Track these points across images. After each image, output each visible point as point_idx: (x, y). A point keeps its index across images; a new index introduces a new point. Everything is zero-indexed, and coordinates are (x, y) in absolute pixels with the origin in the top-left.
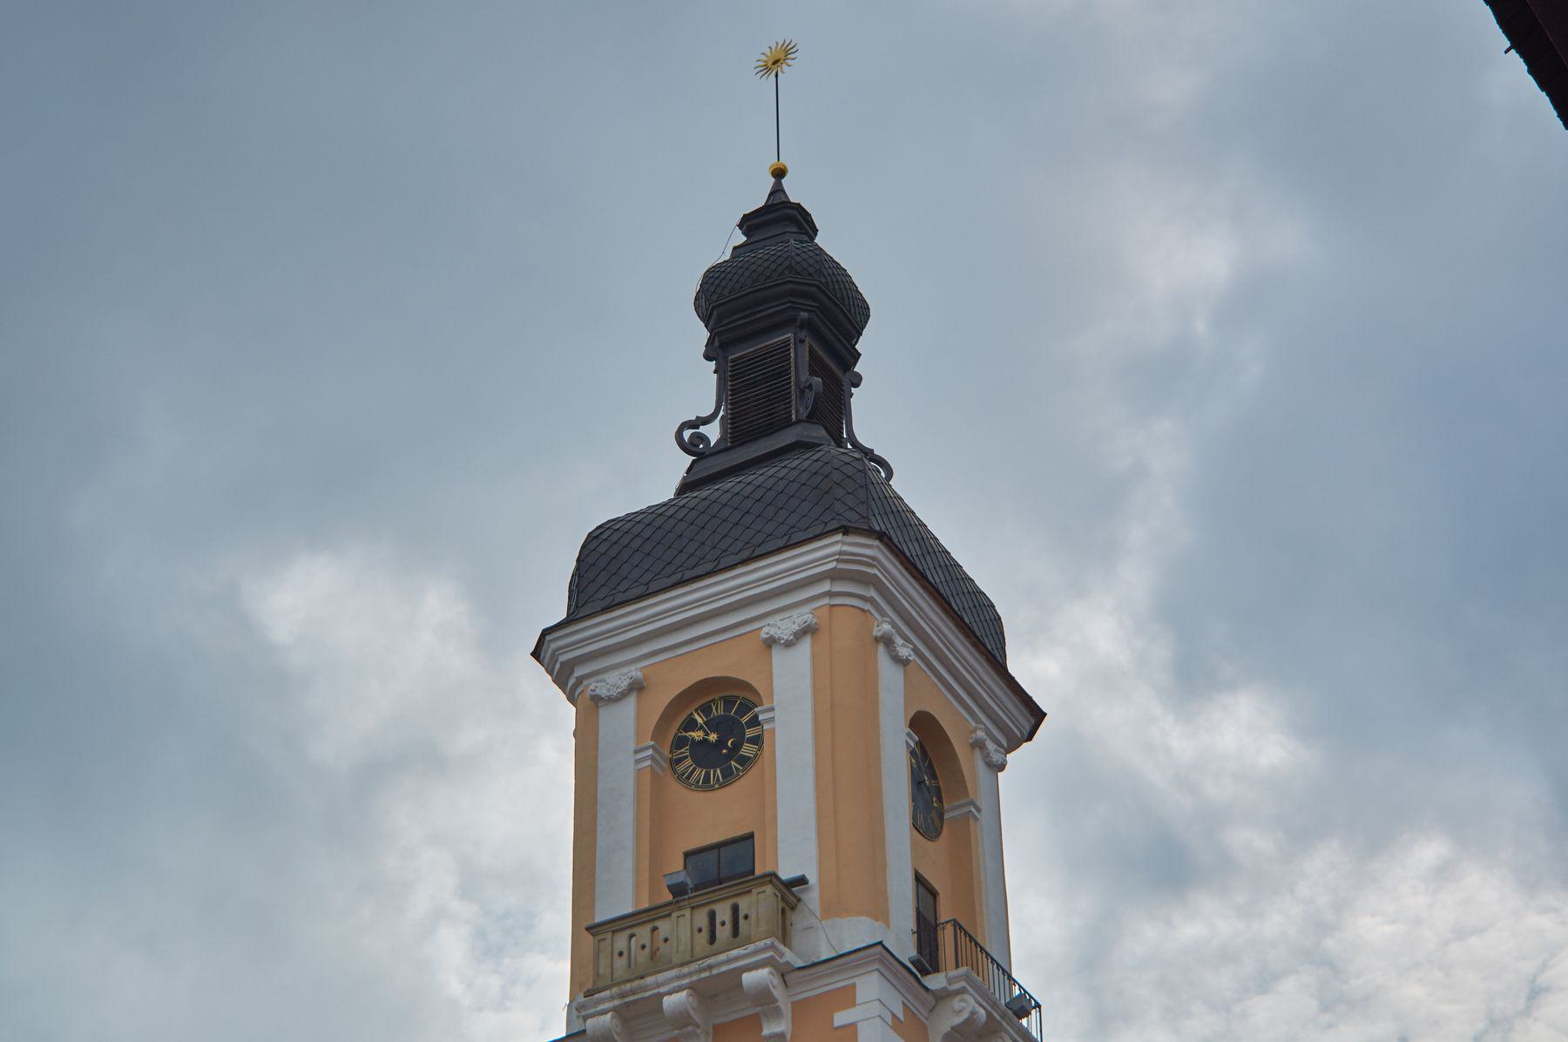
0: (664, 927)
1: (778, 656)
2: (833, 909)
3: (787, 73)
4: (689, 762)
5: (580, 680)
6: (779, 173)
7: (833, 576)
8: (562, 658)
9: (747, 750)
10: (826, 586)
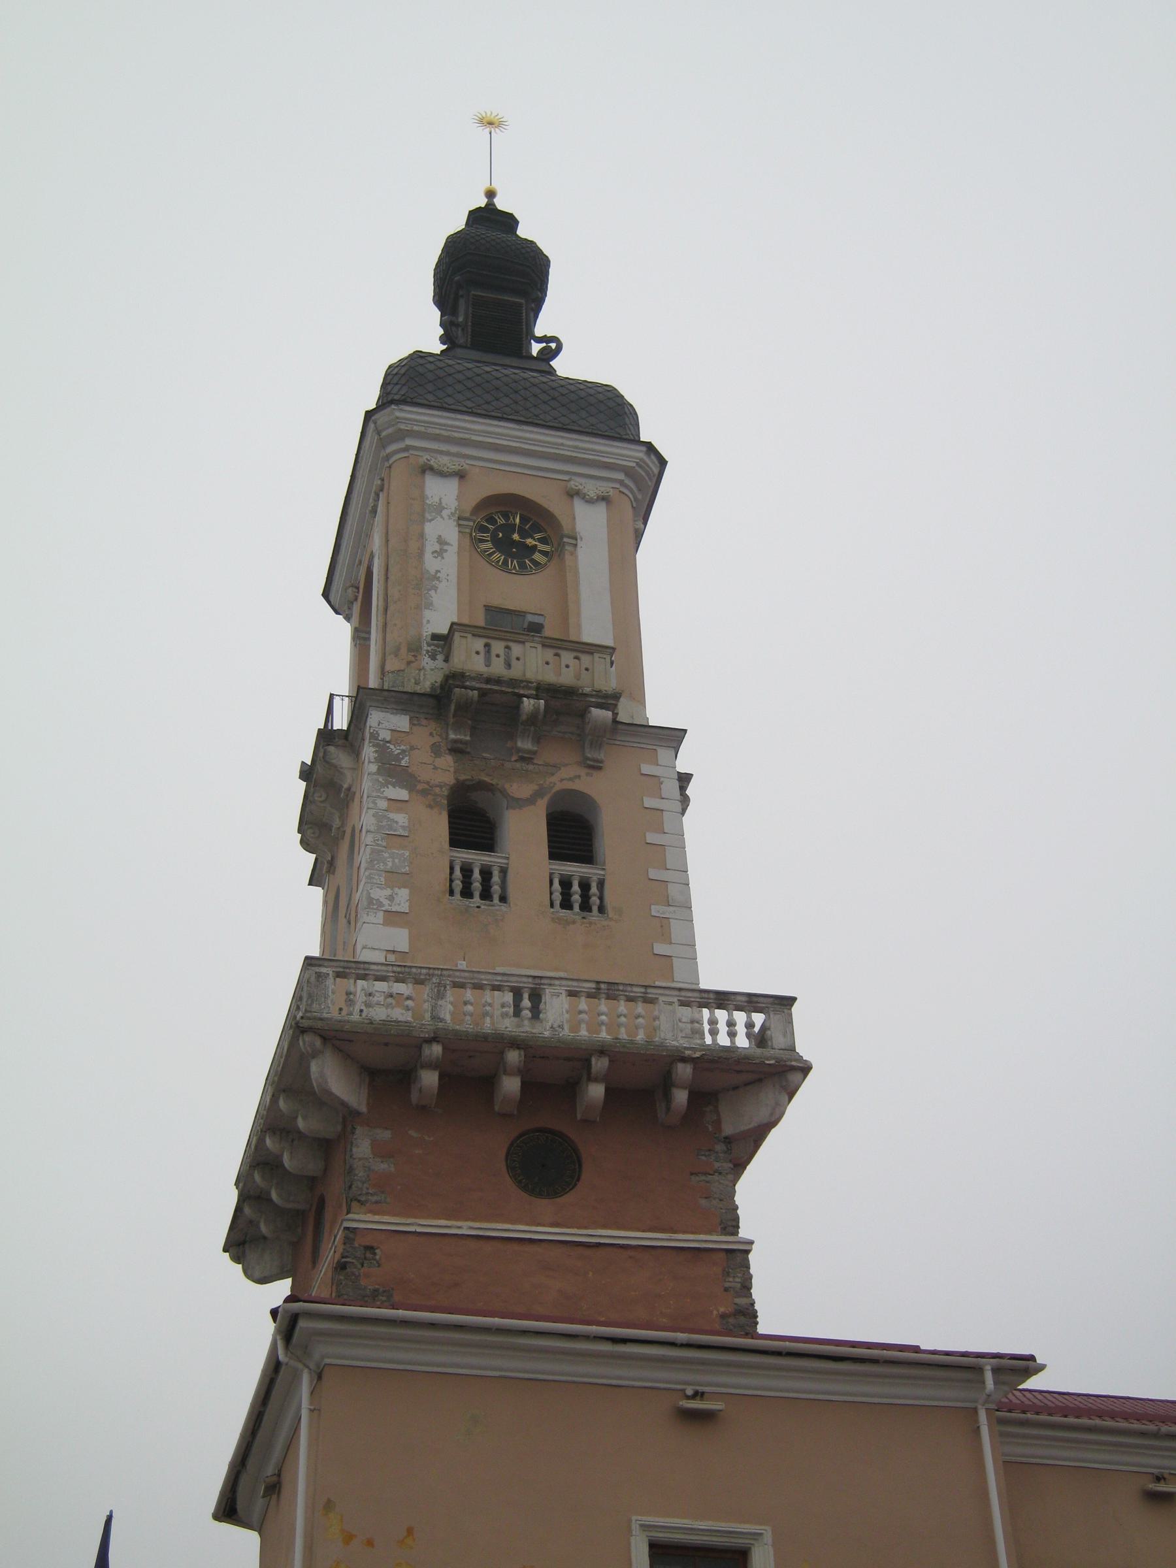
0: (516, 649)
1: (579, 507)
3: (497, 135)
4: (489, 545)
5: (407, 449)
6: (491, 194)
8: (403, 427)
9: (537, 557)
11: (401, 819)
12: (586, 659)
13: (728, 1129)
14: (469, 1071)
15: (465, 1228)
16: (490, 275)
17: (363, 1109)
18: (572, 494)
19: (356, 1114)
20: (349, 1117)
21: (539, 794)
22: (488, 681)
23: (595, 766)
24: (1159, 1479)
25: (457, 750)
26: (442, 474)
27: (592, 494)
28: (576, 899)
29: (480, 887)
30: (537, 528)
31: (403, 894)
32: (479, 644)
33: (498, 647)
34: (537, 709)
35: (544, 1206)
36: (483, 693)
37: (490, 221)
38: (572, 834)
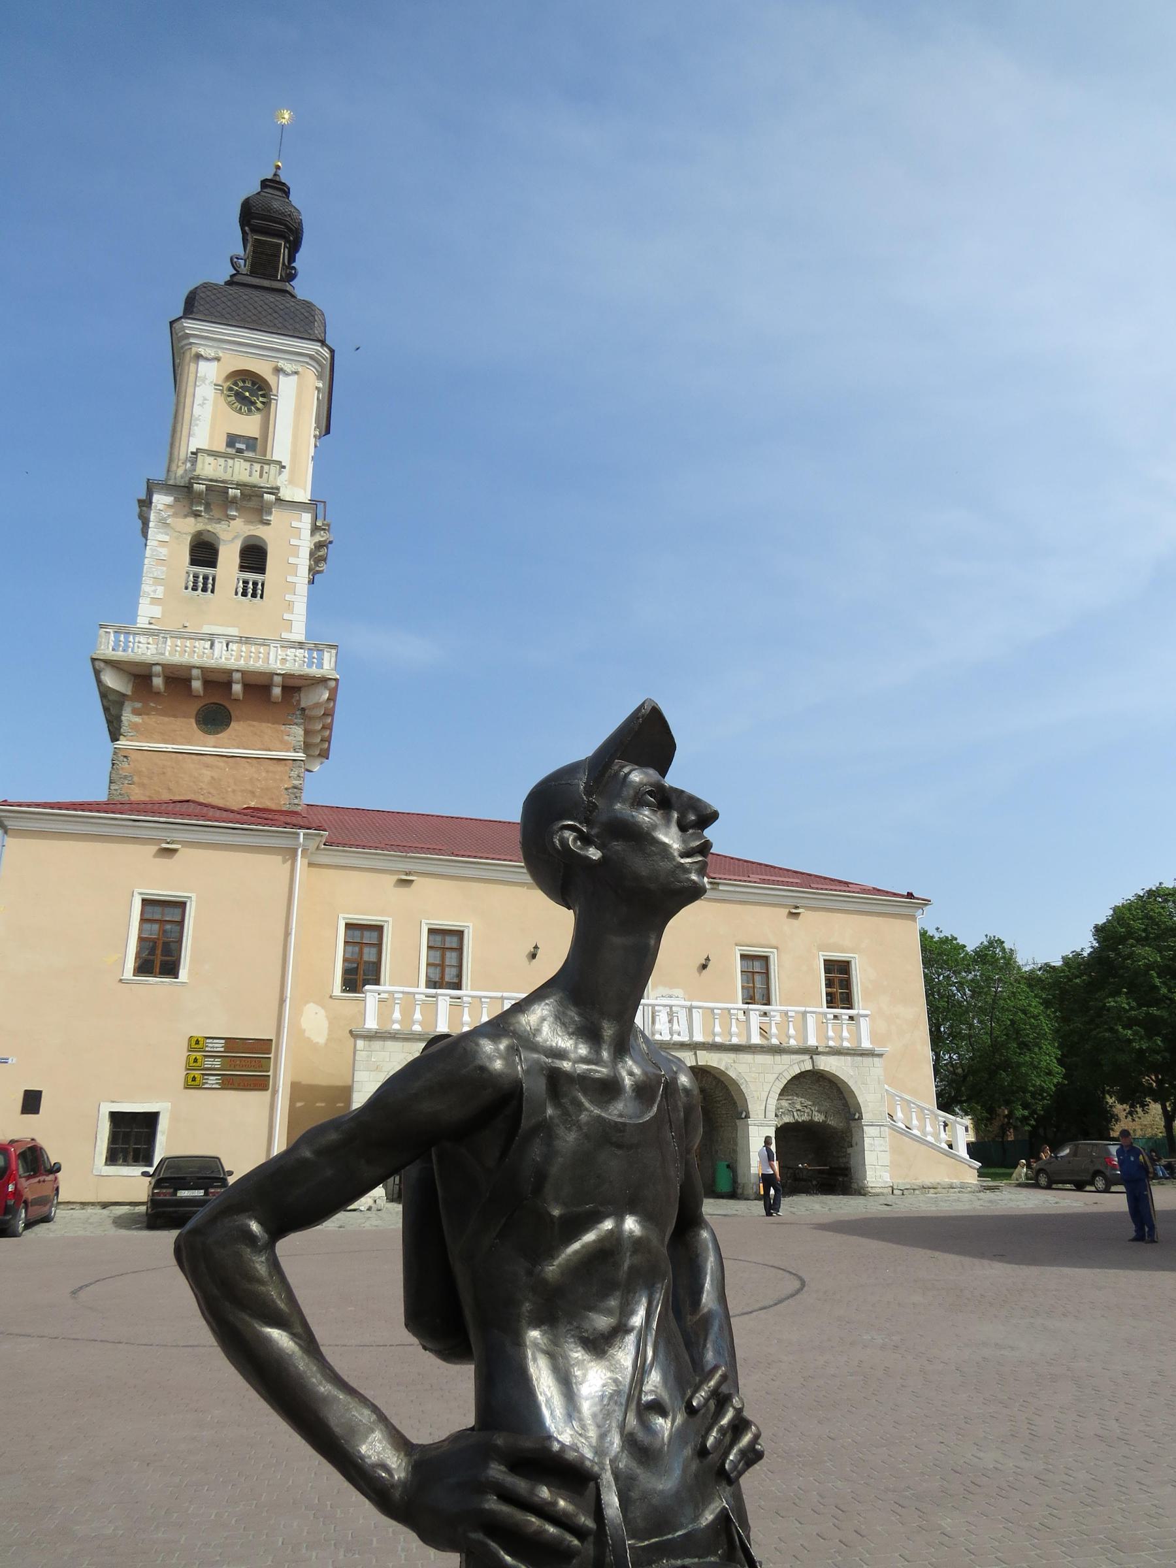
2: (291, 481)
7: (311, 357)
10: (307, 360)
11: (164, 552)
12: (266, 467)
13: (303, 705)
14: (178, 679)
15: (170, 747)
17: (129, 693)
18: (278, 371)
19: (124, 695)
21: (235, 538)
22: (211, 480)
23: (268, 523)
25: (197, 515)
26: (207, 359)
27: (289, 371)
28: (252, 591)
30: (260, 388)
31: (160, 589)
32: (210, 459)
33: (221, 461)
34: (235, 497)
35: (211, 739)
36: (208, 488)
37: (274, 185)
38: (254, 557)
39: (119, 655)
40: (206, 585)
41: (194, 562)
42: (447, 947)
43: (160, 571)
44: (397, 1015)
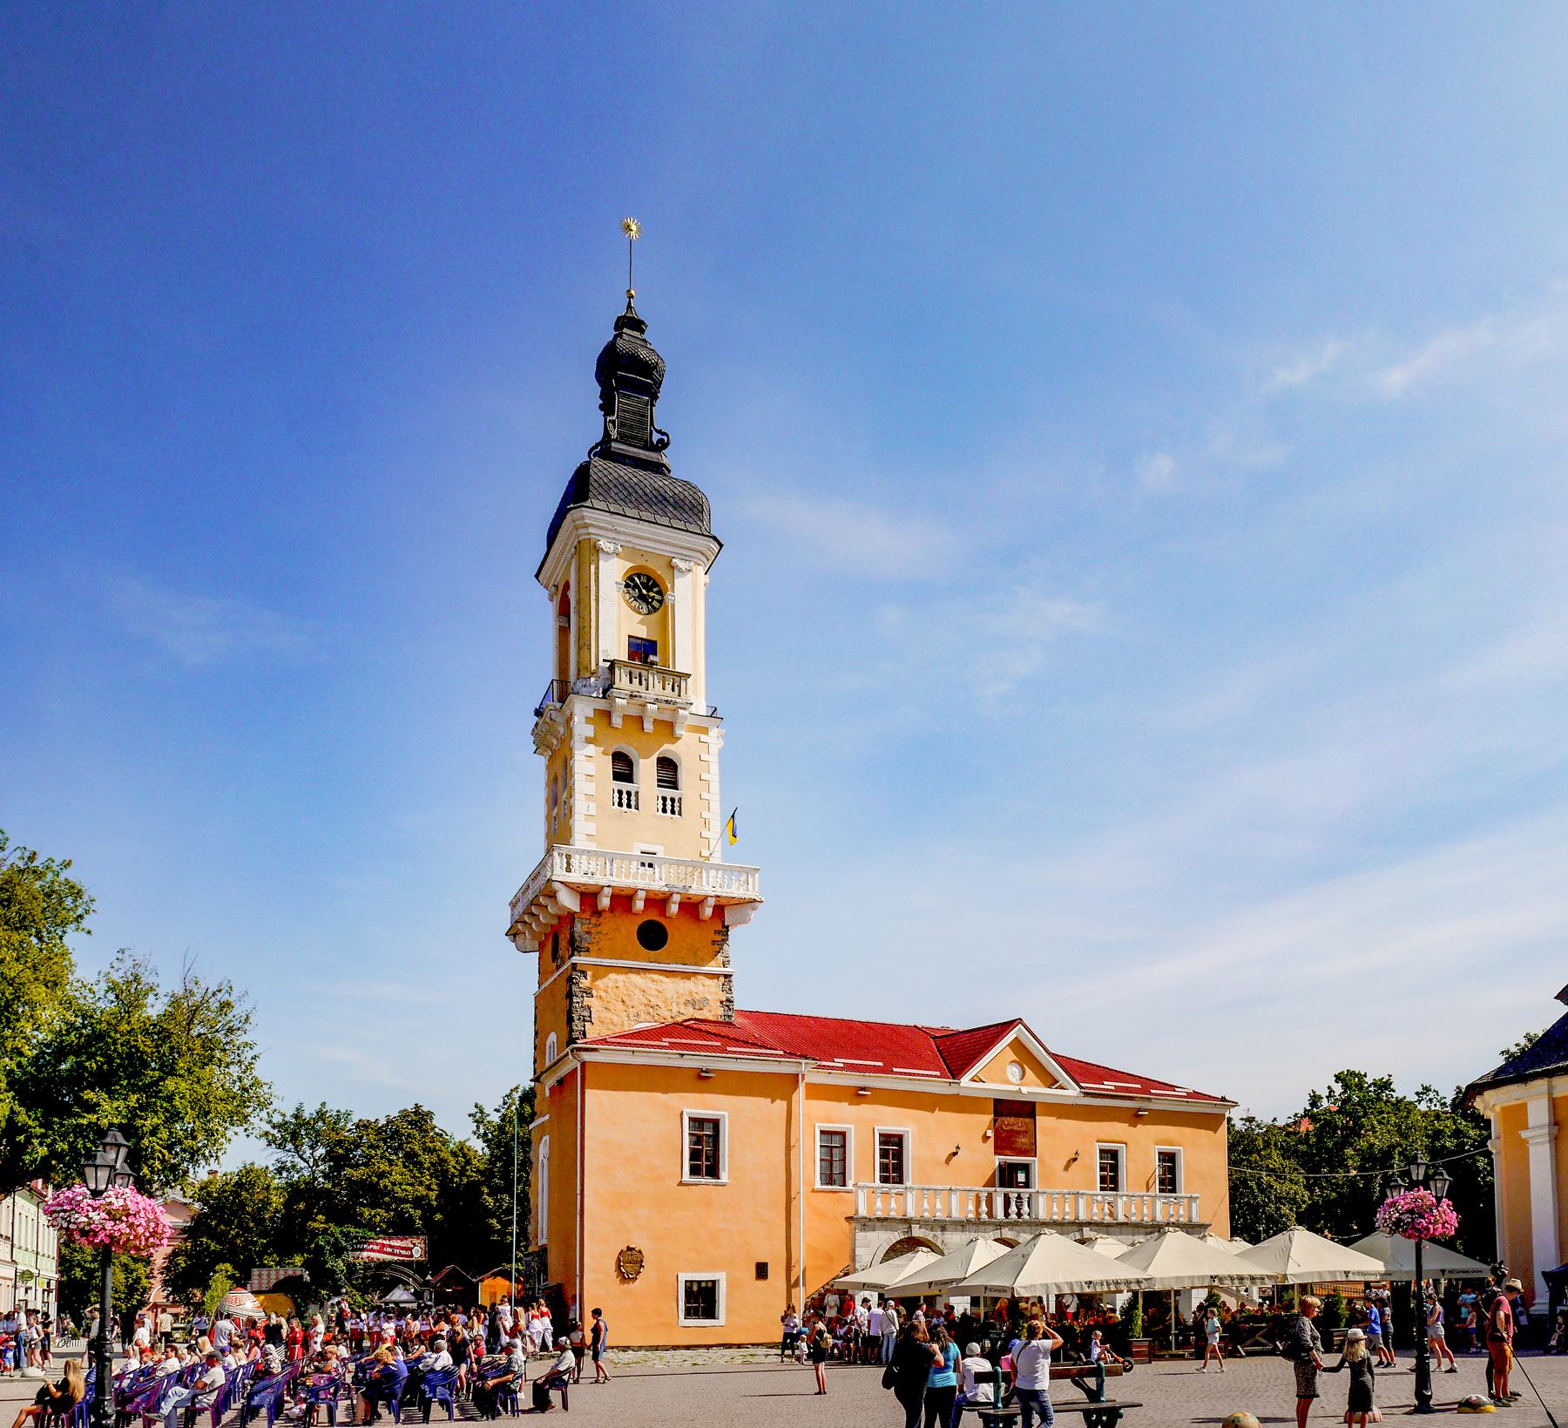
11: (590, 768)
14: (622, 900)
16: (626, 374)
20: (572, 916)
24: (863, 1089)
29: (628, 801)
31: (593, 805)
37: (630, 322)
39: (575, 877)
40: (628, 801)
41: (617, 777)
42: (892, 1146)
43: (590, 788)
44: (879, 1204)
